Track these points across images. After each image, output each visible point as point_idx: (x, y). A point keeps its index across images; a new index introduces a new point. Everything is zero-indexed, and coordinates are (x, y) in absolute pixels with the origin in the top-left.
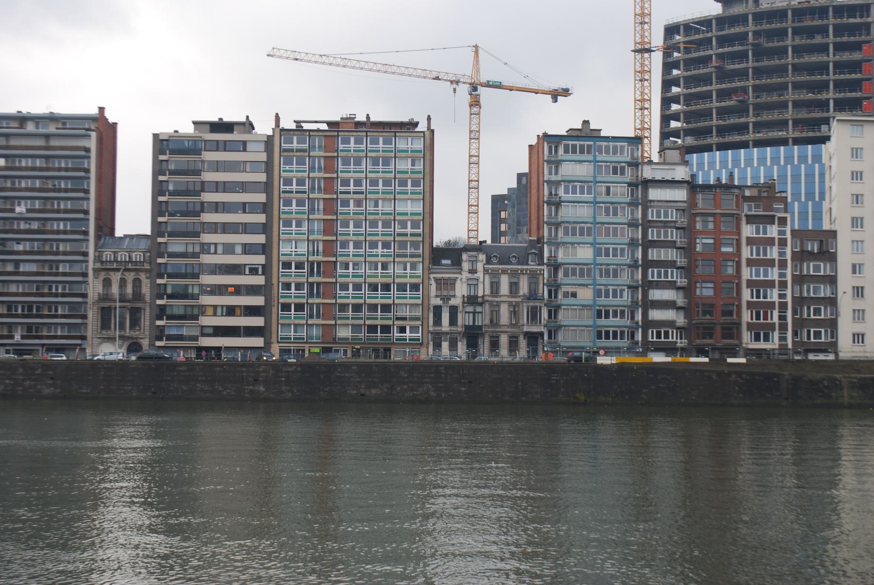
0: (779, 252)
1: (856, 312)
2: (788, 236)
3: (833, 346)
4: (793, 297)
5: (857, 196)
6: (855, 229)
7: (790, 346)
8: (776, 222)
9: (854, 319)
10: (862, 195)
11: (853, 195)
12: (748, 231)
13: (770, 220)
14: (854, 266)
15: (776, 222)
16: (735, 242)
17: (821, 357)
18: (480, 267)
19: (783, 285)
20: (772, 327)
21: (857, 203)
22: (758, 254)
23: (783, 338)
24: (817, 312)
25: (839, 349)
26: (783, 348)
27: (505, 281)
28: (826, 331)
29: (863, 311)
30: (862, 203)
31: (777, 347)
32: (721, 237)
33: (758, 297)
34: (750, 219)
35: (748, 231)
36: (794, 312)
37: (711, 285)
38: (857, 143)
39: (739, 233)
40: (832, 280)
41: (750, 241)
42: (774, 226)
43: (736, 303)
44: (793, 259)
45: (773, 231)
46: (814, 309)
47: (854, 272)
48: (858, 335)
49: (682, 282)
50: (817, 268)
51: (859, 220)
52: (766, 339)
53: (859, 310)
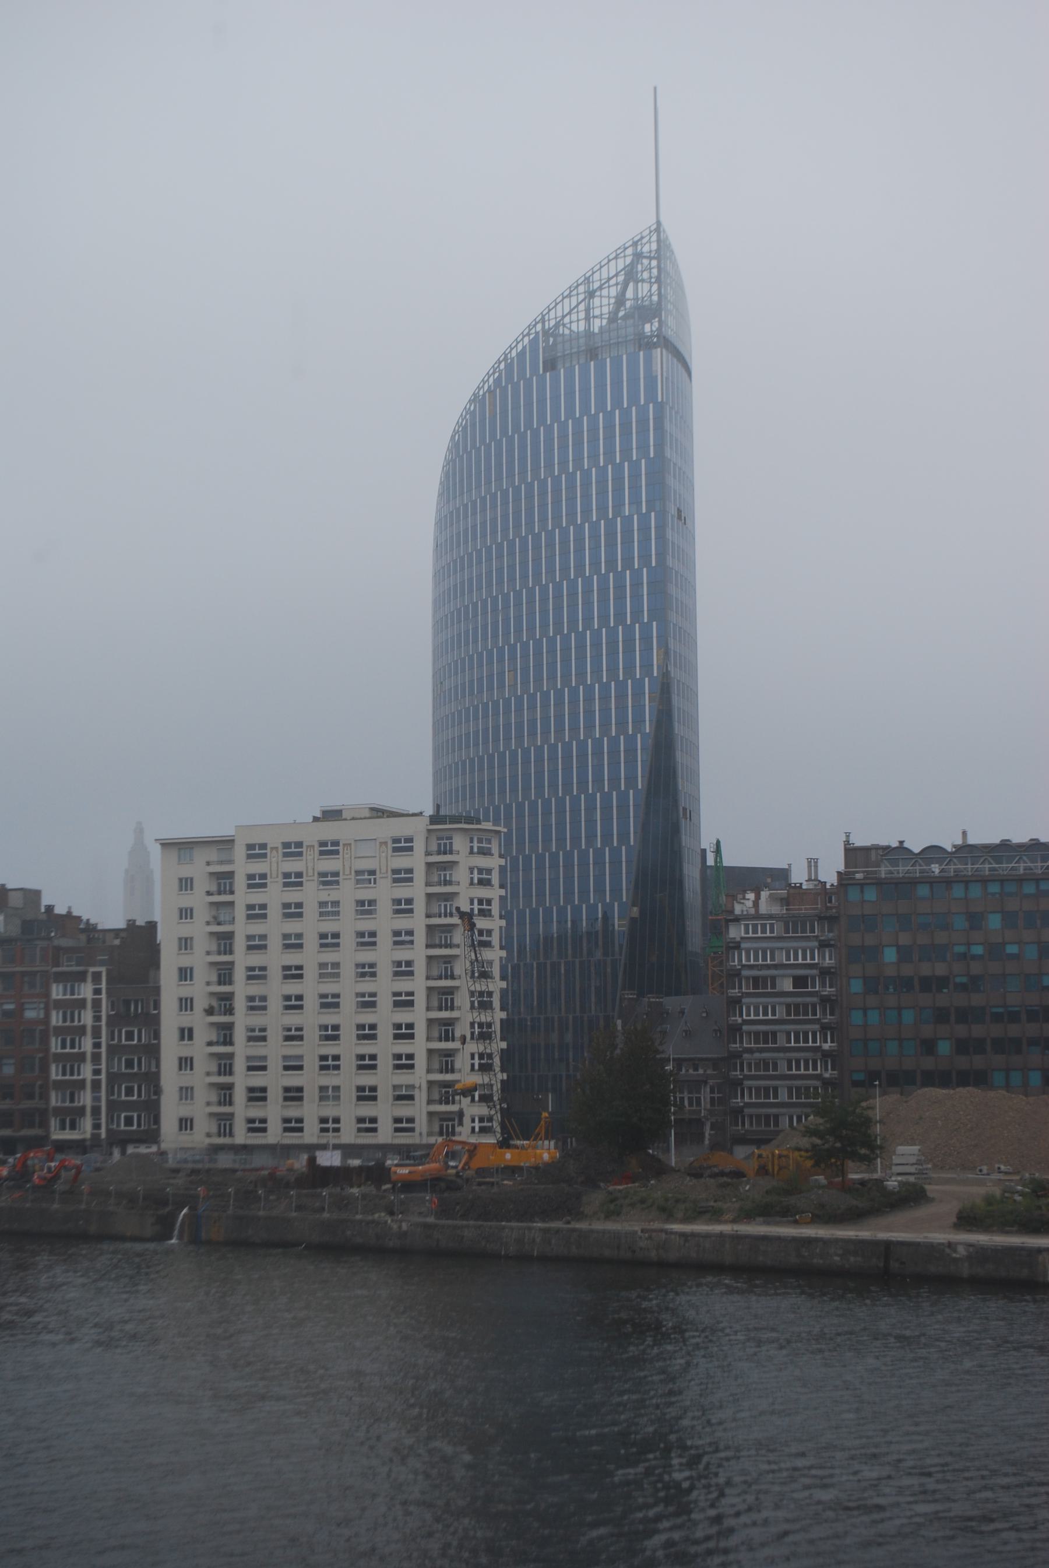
0: (94, 1017)
1: (184, 1090)
2: (104, 996)
3: (152, 1136)
4: (108, 1074)
5: (186, 939)
6: (183, 983)
7: (103, 1136)
8: (89, 979)
9: (181, 1099)
10: (192, 938)
11: (180, 939)
12: (57, 992)
13: (81, 977)
14: (182, 1030)
15: (89, 979)
16: (42, 1006)
17: (143, 1150)
19: (96, 1058)
20: (81, 1111)
21: (186, 949)
22: (65, 1020)
23: (97, 1126)
24: (129, 1092)
25: (162, 1137)
26: (95, 1137)
28: (139, 1117)
29: (192, 1088)
30: (191, 949)
31: (88, 1136)
32: (23, 1001)
33: (64, 1074)
34: (60, 977)
35: (57, 992)
36: (110, 1091)
37: (12, 1061)
38: (186, 871)
39: (47, 995)
40: (153, 1051)
41: (59, 1004)
42: (83, 984)
43: (39, 1083)
44: (108, 1024)
45: (86, 991)
46: (126, 1087)
47: (182, 1038)
48: (186, 1120)
50: (130, 1036)
51: (189, 971)
52: (73, 1127)
53: (187, 1088)
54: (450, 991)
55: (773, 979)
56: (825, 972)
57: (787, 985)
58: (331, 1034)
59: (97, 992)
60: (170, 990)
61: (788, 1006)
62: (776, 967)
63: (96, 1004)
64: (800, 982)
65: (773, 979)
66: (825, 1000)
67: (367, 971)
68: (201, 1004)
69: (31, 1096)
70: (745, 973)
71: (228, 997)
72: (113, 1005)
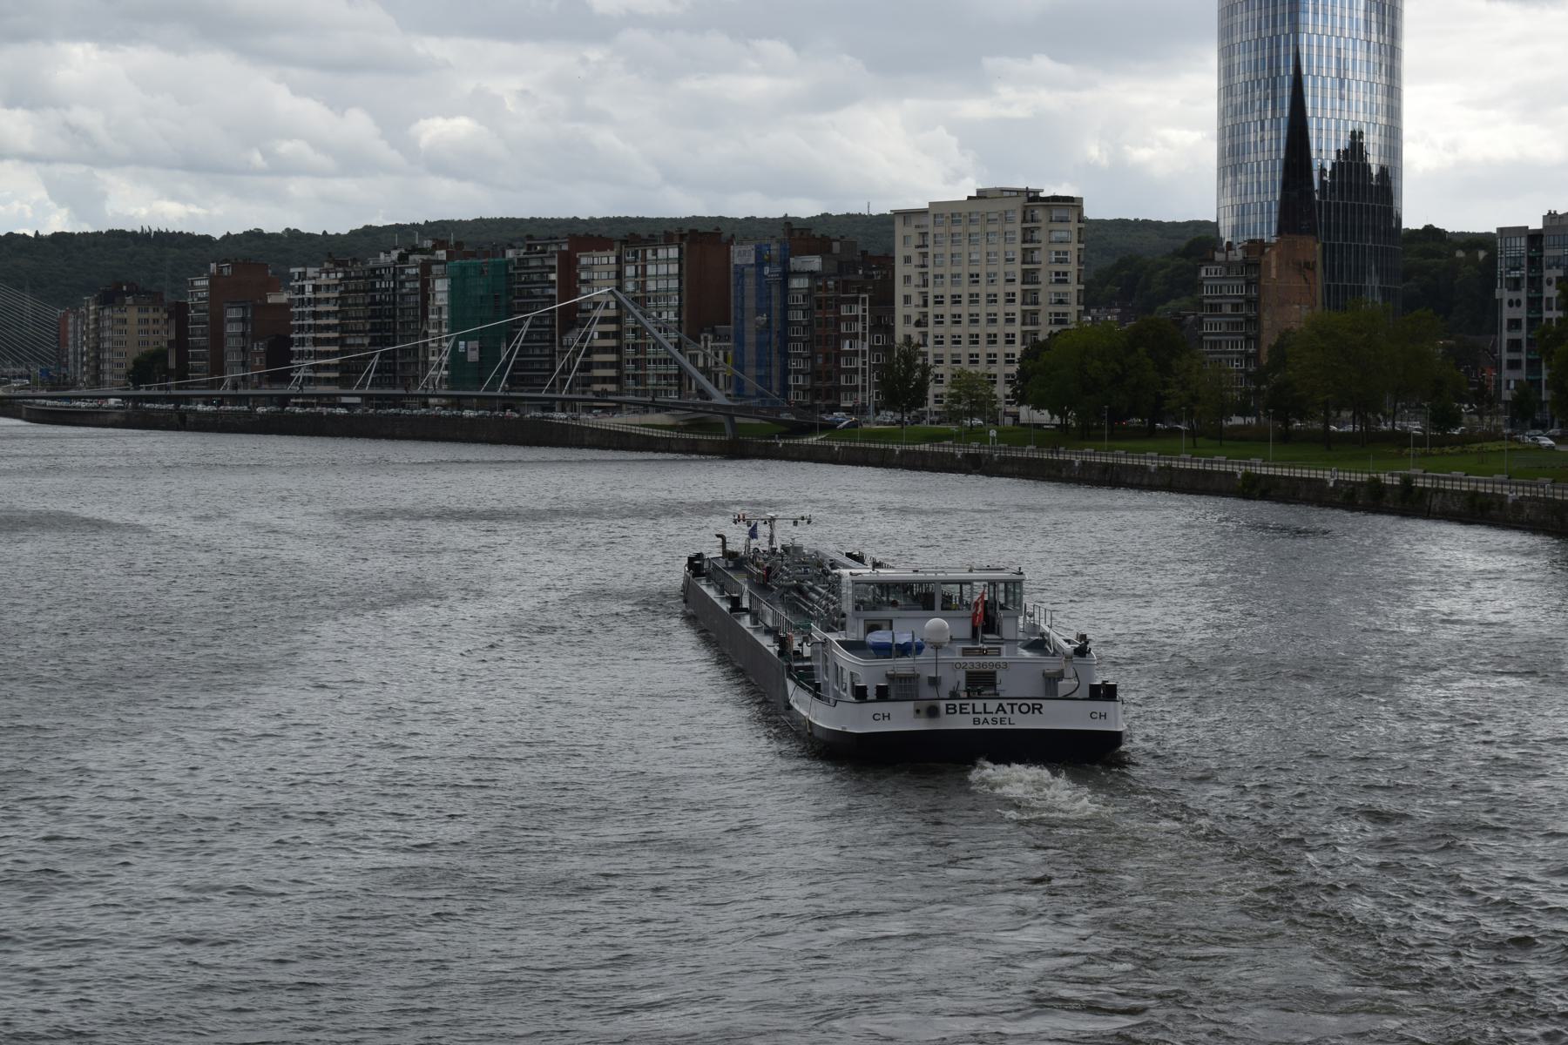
12: (844, 311)
13: (856, 301)
18: (709, 344)
27: (721, 353)
49: (807, 353)
54: (1035, 313)
55: (1220, 305)
56: (1249, 301)
57: (1227, 309)
58: (992, 339)
59: (864, 310)
60: (900, 310)
61: (1228, 323)
62: (1221, 297)
63: (864, 318)
64: (1236, 307)
65: (1220, 305)
66: (1248, 320)
67: (956, 300)
68: (914, 319)
69: (829, 378)
70: (1206, 301)
71: (925, 315)
72: (872, 320)
